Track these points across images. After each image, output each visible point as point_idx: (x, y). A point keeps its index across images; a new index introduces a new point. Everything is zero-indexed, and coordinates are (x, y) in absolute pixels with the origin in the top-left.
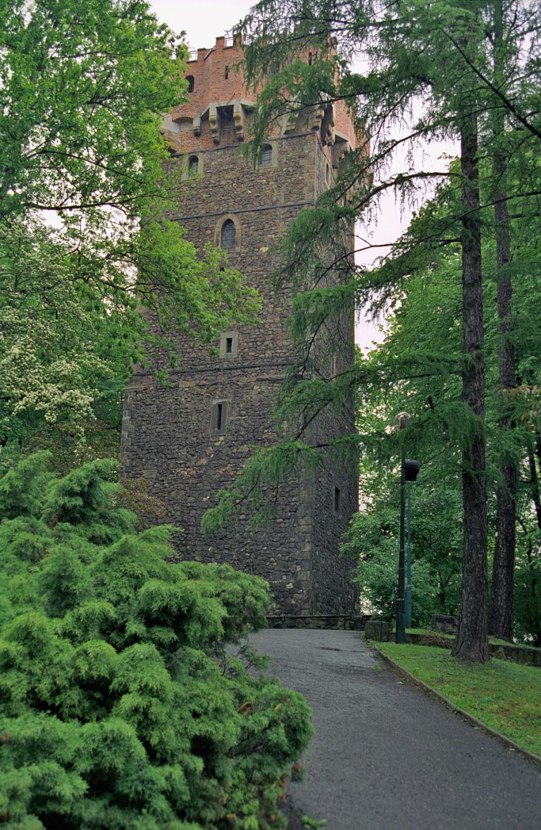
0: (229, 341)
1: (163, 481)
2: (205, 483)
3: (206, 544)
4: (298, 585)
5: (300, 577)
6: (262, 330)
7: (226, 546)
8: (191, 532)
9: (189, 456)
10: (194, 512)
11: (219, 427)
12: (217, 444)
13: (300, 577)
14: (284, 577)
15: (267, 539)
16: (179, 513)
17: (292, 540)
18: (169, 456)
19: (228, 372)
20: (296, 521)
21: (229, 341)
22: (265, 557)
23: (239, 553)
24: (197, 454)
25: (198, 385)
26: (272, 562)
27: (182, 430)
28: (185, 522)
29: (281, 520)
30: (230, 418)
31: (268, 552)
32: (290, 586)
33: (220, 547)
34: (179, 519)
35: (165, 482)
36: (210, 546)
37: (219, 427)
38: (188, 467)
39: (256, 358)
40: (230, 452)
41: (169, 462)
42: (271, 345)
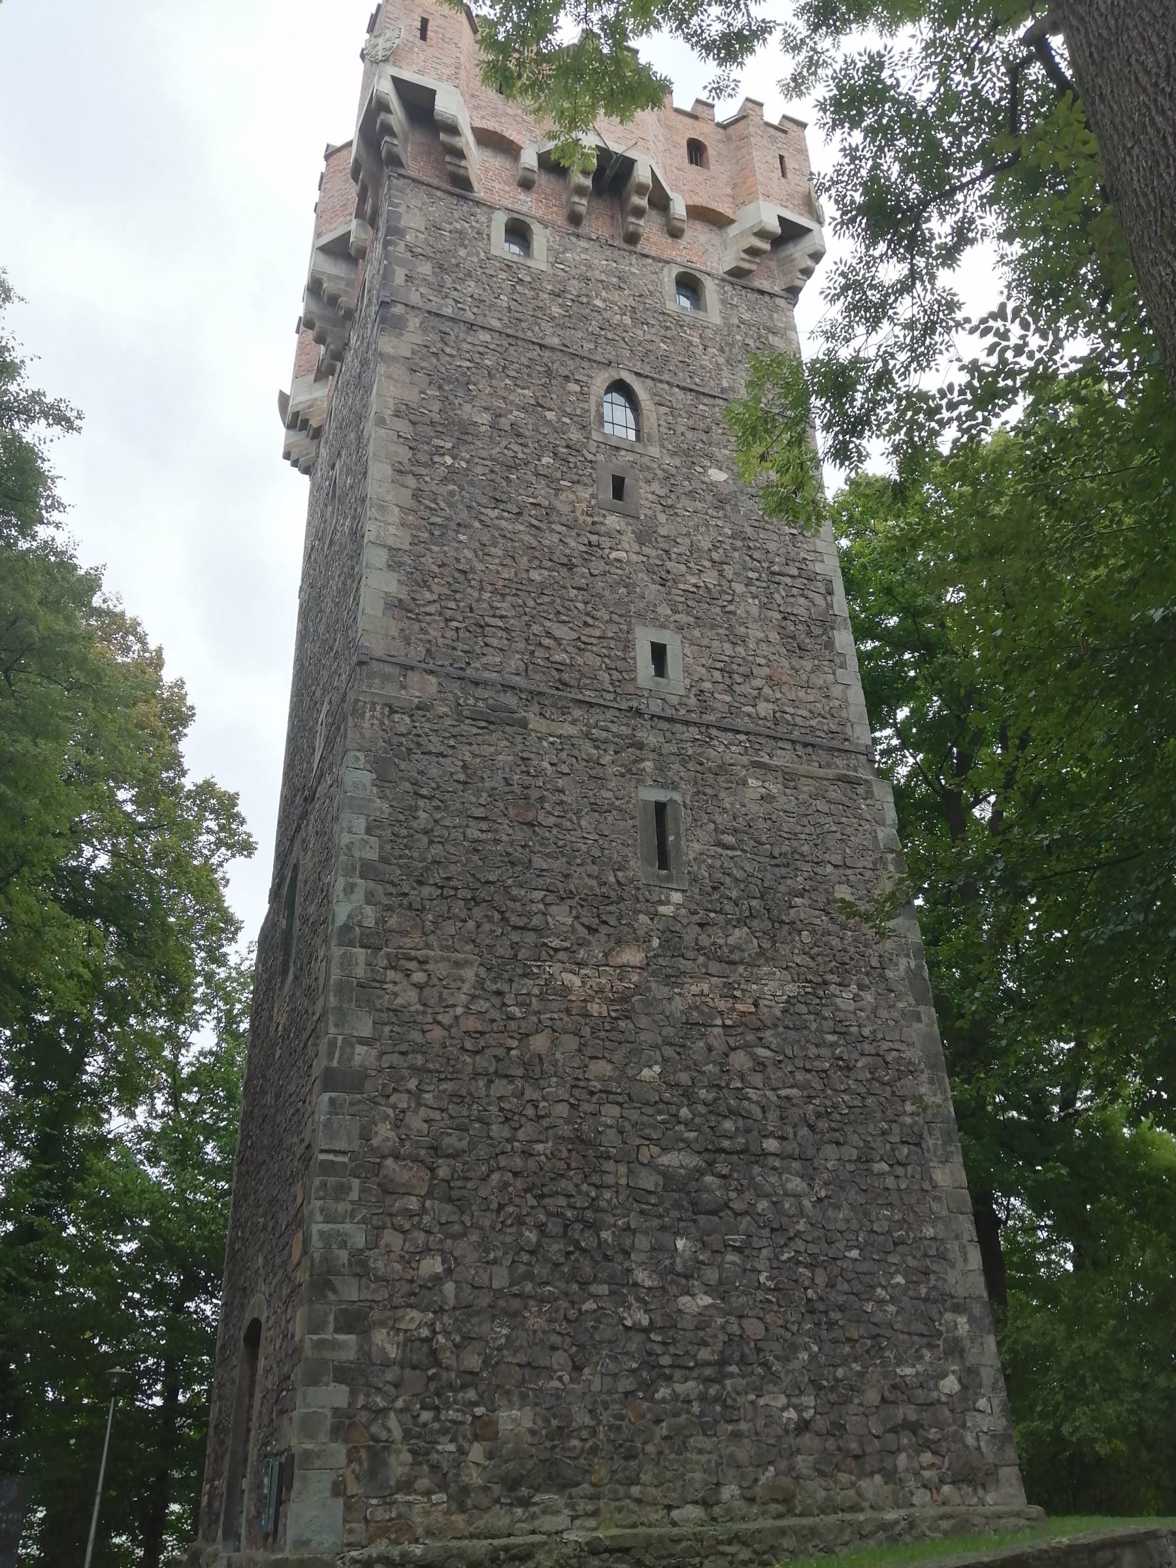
0: (659, 653)
1: (499, 993)
2: (644, 1021)
3: (663, 1228)
4: (970, 1378)
5: (971, 1359)
6: (740, 649)
7: (736, 1239)
8: (610, 1179)
9: (582, 932)
10: (615, 1111)
11: (664, 865)
12: (662, 909)
13: (971, 1359)
14: (927, 1355)
15: (854, 1224)
16: (562, 1110)
17: (929, 1232)
18: (514, 920)
19: (665, 725)
20: (926, 1175)
21: (659, 653)
22: (858, 1287)
23: (775, 1265)
24: (604, 929)
25: (587, 736)
26: (881, 1302)
27: (552, 848)
28: (588, 1143)
29: (885, 1167)
30: (693, 846)
31: (864, 1267)
32: (950, 1384)
33: (715, 1240)
34: (566, 1130)
35: (510, 999)
36: (677, 1234)
37: (664, 865)
38: (581, 965)
39: (733, 711)
40: (705, 941)
41: (515, 937)
42: (767, 690)
